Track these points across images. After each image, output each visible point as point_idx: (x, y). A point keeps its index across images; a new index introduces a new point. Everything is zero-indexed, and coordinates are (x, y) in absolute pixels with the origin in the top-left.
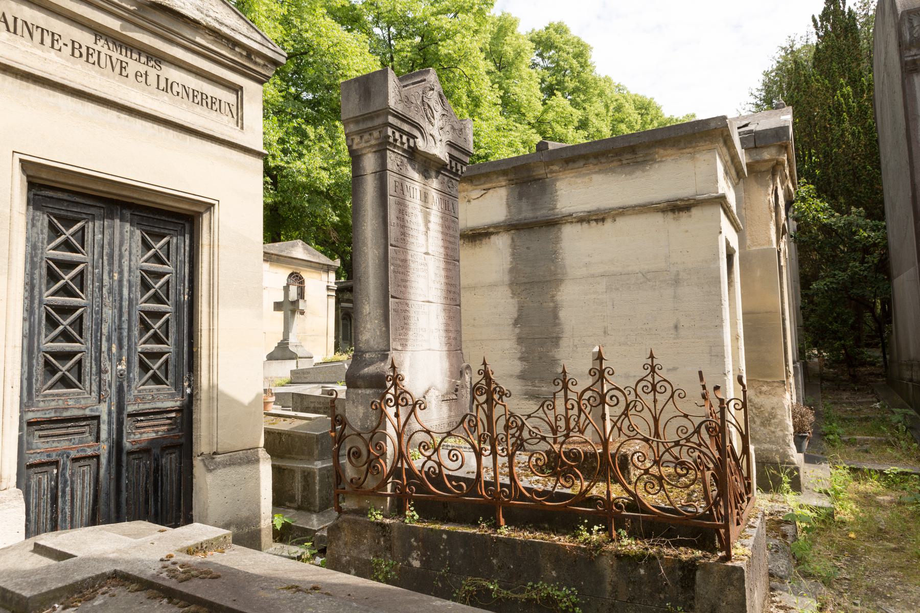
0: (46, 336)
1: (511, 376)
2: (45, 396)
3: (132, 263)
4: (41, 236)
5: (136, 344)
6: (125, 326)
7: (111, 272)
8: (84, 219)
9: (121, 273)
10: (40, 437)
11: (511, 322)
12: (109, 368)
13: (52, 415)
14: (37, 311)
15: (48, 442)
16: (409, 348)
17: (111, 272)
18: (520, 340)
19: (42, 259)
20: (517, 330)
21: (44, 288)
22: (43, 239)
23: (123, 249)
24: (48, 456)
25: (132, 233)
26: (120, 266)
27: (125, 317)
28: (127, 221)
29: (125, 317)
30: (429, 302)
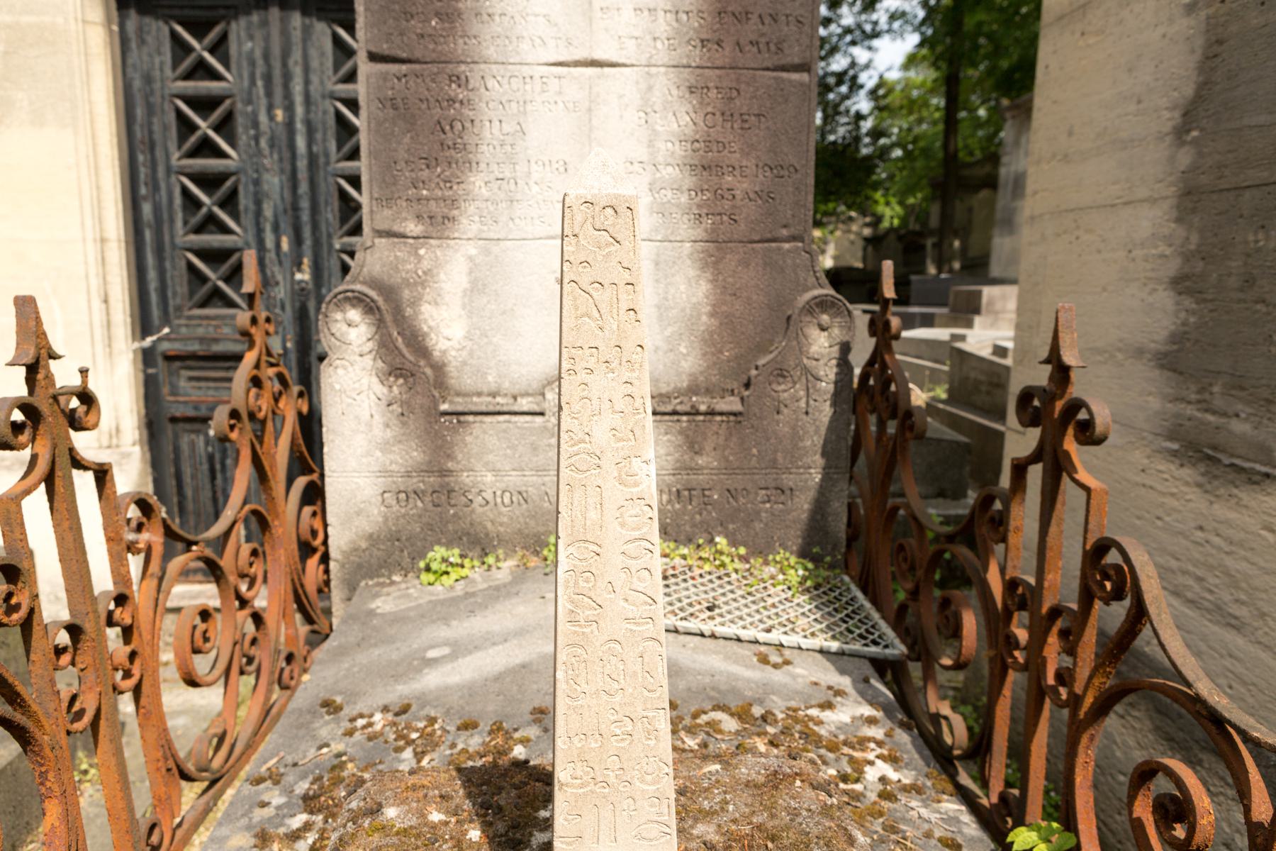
0: (185, 223)
1: (1139, 352)
2: (190, 318)
3: (312, 88)
4: (157, 60)
5: (330, 236)
6: (305, 204)
7: (270, 108)
8: (223, 18)
9: (289, 109)
10: (191, 379)
11: (1169, 120)
12: (279, 278)
13: (195, 347)
14: (163, 185)
15: (200, 388)
16: (469, 223)
17: (270, 108)
18: (1191, 198)
19: (163, 97)
20: (1185, 158)
21: (172, 145)
22: (162, 63)
23: (291, 62)
24: (196, 408)
25: (307, 31)
26: (288, 95)
27: (303, 188)
28: (293, 8)
29: (303, 188)
30: (594, 63)
